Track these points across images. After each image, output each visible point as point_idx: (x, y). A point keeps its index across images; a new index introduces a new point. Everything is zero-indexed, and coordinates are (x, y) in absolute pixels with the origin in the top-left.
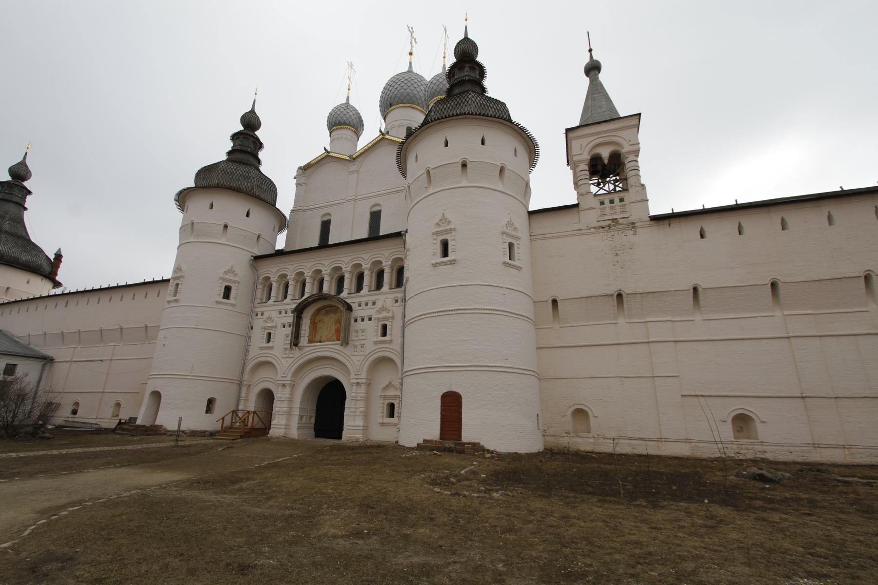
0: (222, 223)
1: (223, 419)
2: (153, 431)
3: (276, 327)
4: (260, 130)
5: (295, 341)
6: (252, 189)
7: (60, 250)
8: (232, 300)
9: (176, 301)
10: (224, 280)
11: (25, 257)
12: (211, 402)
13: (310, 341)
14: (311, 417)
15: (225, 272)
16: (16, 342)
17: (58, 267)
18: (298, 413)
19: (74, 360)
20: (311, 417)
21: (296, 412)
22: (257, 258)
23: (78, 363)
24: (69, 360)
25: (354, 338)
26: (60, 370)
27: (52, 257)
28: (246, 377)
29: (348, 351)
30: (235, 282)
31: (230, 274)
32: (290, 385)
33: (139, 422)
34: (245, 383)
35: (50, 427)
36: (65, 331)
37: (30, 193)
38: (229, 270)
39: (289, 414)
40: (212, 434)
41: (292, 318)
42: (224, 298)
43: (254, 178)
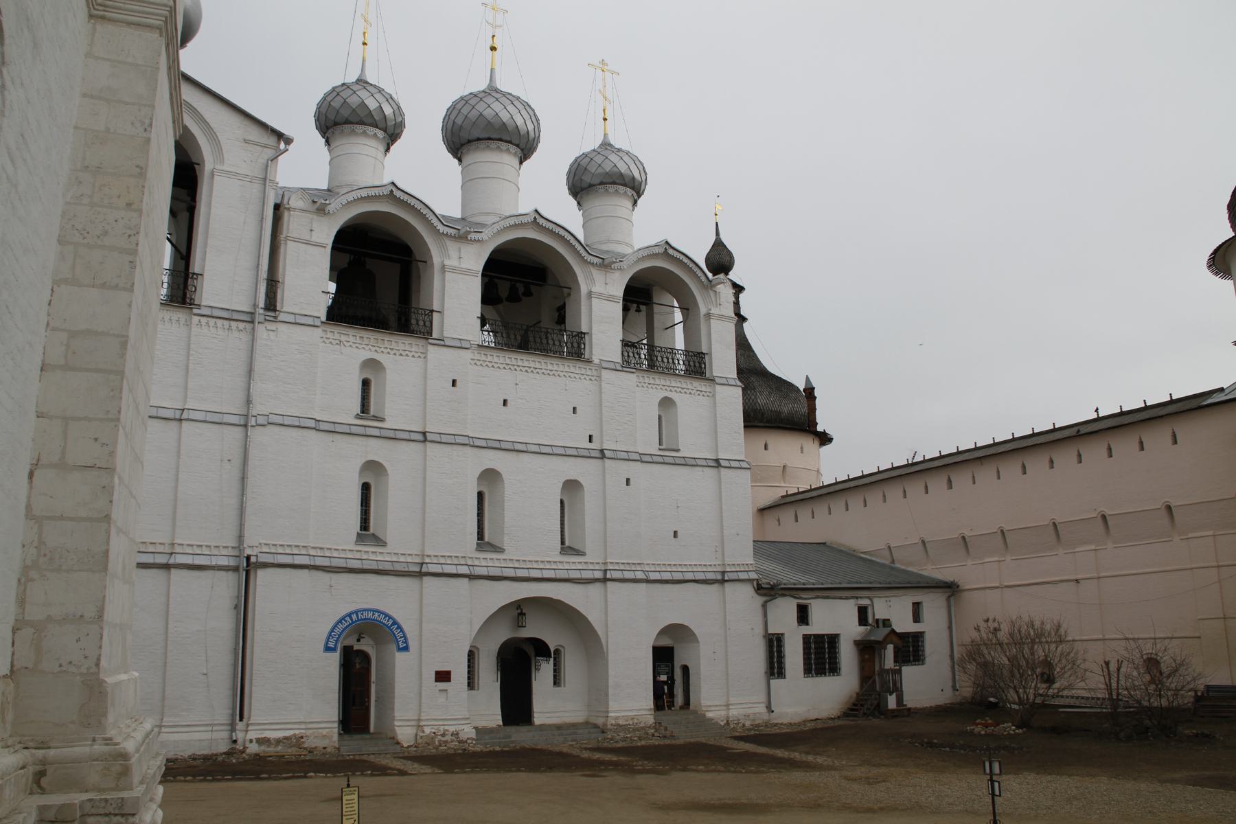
7: (808, 379)
19: (1006, 584)
23: (1017, 588)
24: (997, 585)
36: (967, 533)
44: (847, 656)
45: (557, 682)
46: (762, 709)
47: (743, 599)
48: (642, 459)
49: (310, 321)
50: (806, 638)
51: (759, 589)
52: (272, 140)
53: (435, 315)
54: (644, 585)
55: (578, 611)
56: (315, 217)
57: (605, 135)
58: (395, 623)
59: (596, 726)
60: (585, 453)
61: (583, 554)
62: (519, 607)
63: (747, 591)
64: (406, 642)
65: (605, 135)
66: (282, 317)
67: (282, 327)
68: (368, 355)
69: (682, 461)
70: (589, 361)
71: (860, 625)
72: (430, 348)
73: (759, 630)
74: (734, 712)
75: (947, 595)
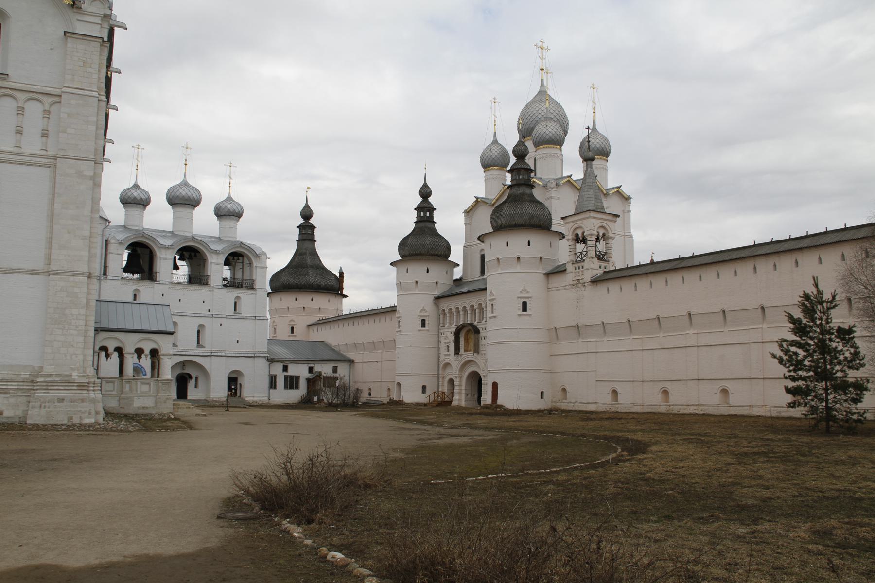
0: (414, 281)
1: (429, 396)
2: (400, 403)
3: (450, 342)
4: (433, 193)
5: (457, 351)
6: (428, 252)
8: (426, 328)
9: (400, 331)
10: (421, 316)
11: (324, 282)
12: (424, 387)
13: (466, 351)
14: (474, 395)
15: (421, 312)
16: (333, 350)
17: (343, 282)
18: (464, 393)
20: (474, 395)
21: (463, 392)
22: (437, 298)
25: (482, 350)
26: (358, 367)
27: (338, 275)
28: (441, 372)
29: (479, 357)
30: (426, 316)
31: (424, 312)
32: (459, 377)
33: (394, 399)
34: (441, 376)
35: (360, 403)
37: (315, 228)
38: (422, 310)
39: (460, 393)
40: (425, 404)
41: (453, 337)
42: (422, 327)
43: (428, 244)
44: (303, 384)
45: (196, 386)
46: (266, 399)
47: (262, 364)
48: (227, 317)
49: (117, 278)
50: (286, 377)
51: (268, 360)
52: (104, 222)
53: (158, 273)
54: (224, 358)
55: (201, 365)
56: (118, 245)
57: (230, 193)
58: (142, 367)
59: (207, 400)
60: (206, 316)
61: (205, 347)
62: (184, 363)
63: (264, 360)
64: (146, 373)
65: (230, 193)
66: (108, 278)
67: (108, 280)
68: (135, 288)
69: (242, 317)
70: (210, 286)
71: (309, 373)
72: (155, 285)
73: (267, 373)
74: (255, 399)
75: (349, 364)
